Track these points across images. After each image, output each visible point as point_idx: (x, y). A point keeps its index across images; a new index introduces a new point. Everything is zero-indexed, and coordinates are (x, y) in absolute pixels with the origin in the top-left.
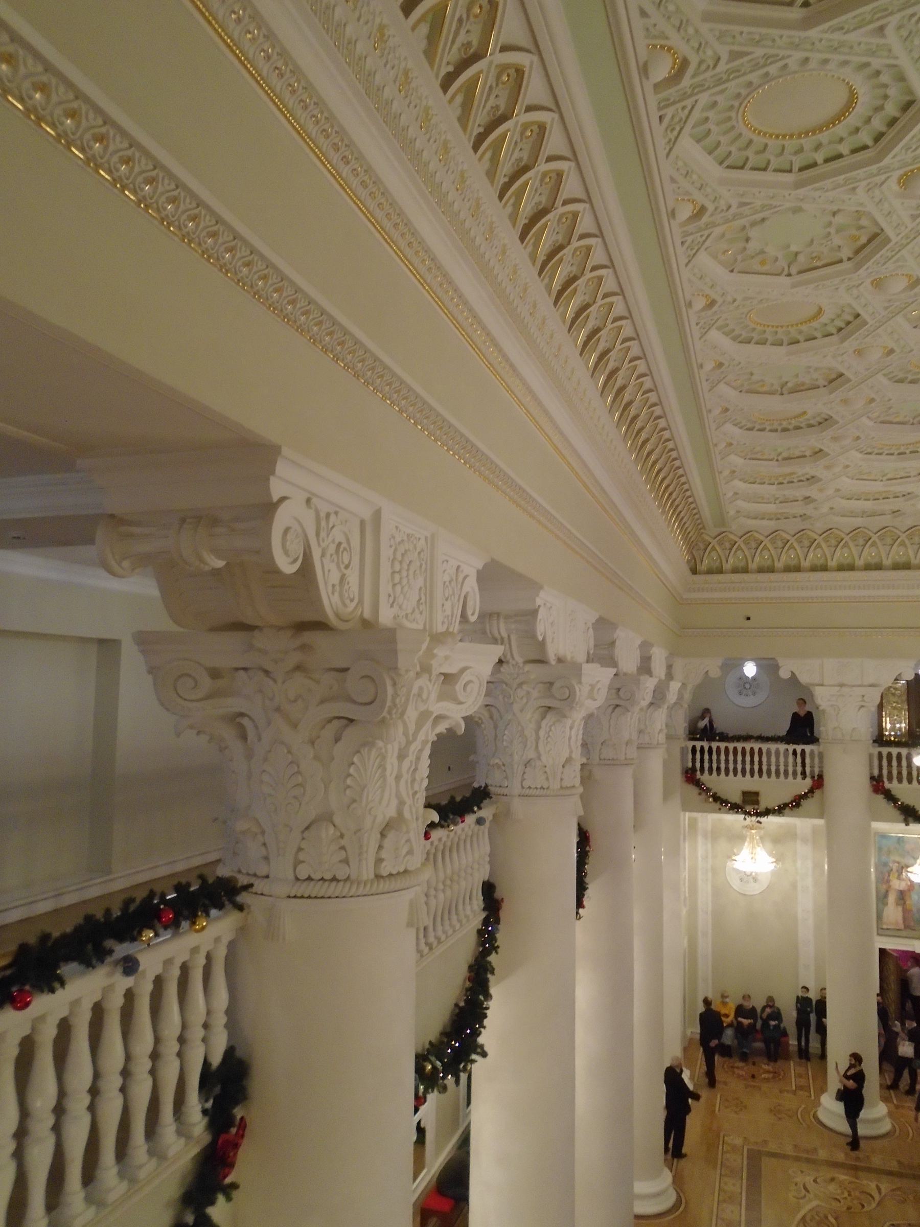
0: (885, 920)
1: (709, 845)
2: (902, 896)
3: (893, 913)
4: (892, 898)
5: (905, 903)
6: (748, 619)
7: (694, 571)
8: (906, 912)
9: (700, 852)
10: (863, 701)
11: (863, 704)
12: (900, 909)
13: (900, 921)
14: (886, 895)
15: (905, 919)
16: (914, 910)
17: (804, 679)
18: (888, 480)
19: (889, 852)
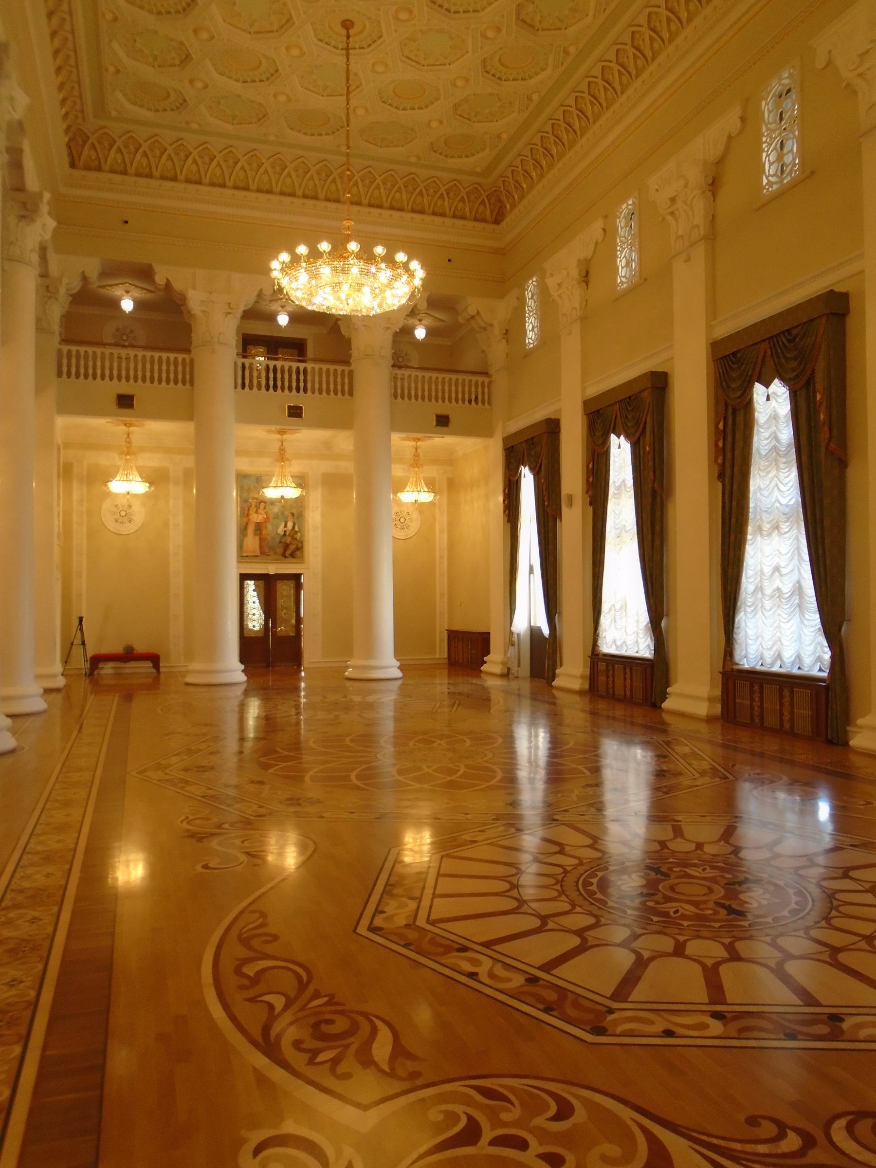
1: (85, 489)
2: (259, 527)
3: (252, 542)
4: (251, 529)
5: (261, 534)
6: (126, 222)
7: (73, 165)
8: (261, 540)
9: (75, 497)
10: (230, 308)
11: (230, 311)
12: (257, 538)
13: (258, 549)
15: (261, 547)
16: (269, 538)
17: (177, 286)
18: (257, 33)
19: (249, 490)
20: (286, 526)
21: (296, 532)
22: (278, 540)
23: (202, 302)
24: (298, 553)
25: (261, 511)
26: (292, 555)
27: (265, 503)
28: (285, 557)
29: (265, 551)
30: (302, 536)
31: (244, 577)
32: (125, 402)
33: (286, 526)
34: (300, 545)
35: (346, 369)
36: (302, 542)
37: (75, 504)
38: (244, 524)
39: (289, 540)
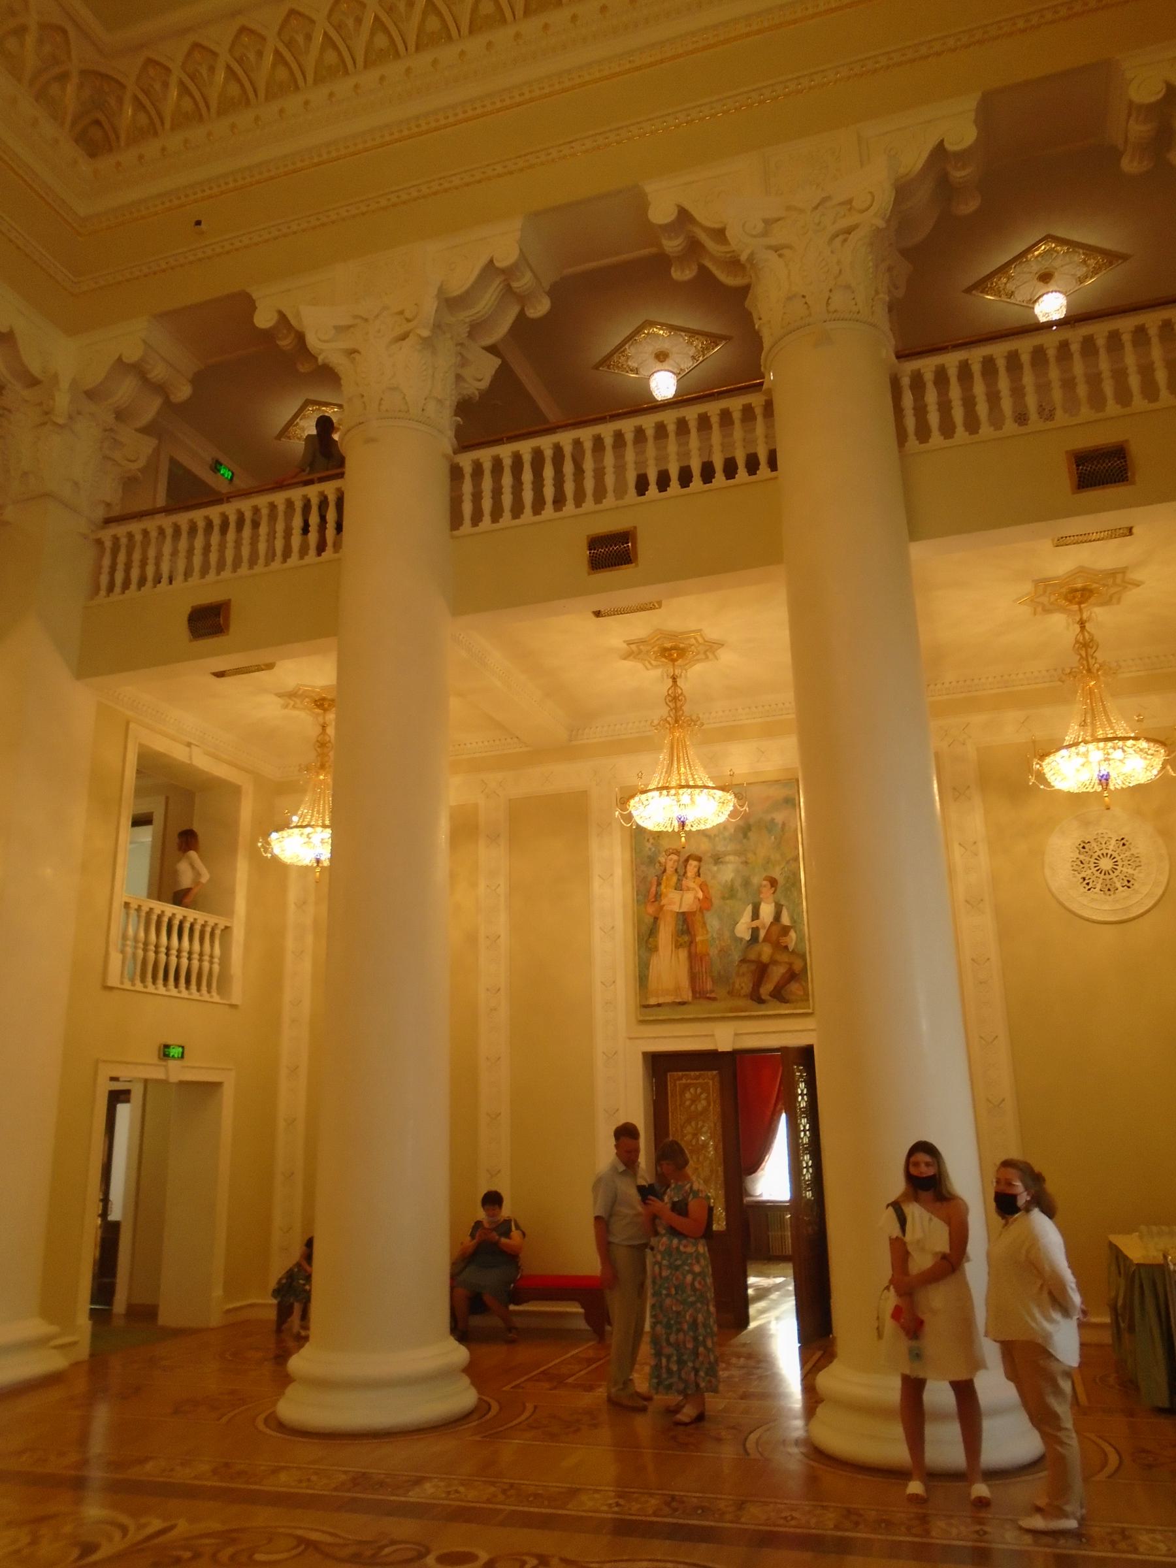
0: (653, 984)
2: (686, 924)
3: (670, 967)
4: (665, 935)
5: (692, 942)
6: (198, 223)
8: (695, 959)
11: (407, 327)
12: (683, 954)
13: (685, 983)
14: (653, 931)
15: (693, 978)
16: (713, 952)
20: (756, 915)
21: (785, 930)
22: (736, 956)
23: (340, 330)
24: (794, 987)
25: (689, 882)
26: (779, 995)
27: (699, 859)
28: (761, 1001)
29: (704, 990)
30: (801, 939)
31: (661, 1066)
32: (208, 621)
33: (756, 915)
34: (797, 966)
35: (756, 400)
36: (803, 957)
37: (292, 908)
38: (649, 920)
39: (766, 952)
